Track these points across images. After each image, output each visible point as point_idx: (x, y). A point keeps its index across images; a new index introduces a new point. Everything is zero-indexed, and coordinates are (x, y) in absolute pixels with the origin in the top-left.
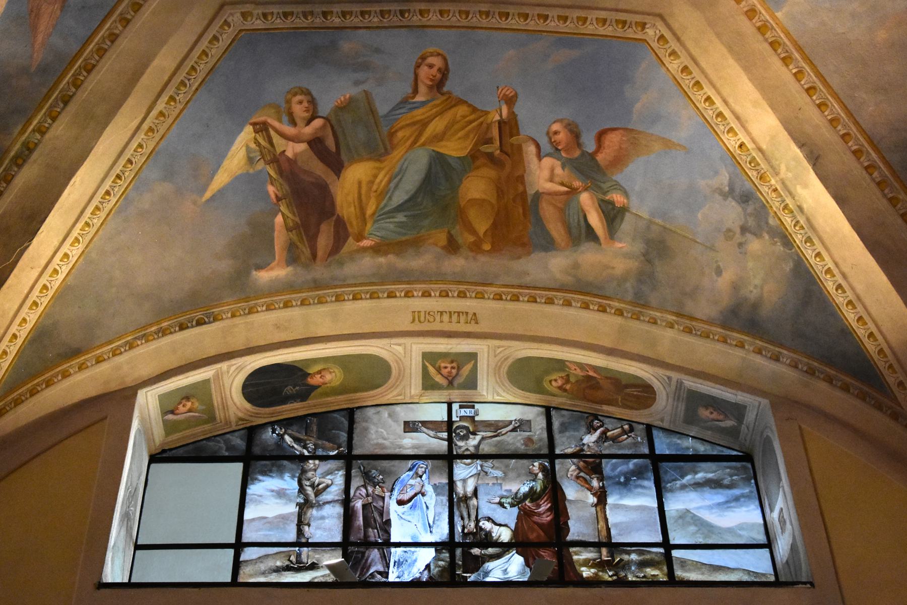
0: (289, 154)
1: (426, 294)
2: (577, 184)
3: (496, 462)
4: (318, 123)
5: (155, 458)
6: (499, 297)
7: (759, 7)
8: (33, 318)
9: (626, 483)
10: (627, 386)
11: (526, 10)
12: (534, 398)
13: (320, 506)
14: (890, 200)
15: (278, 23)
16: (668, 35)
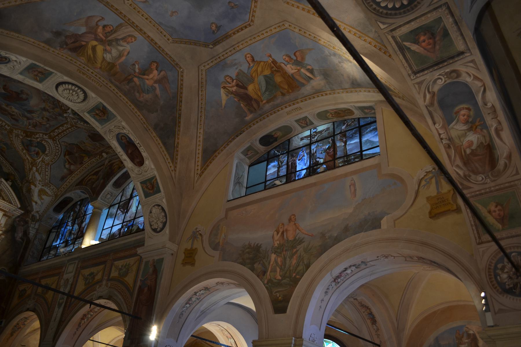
0: (234, 90)
1: (286, 107)
2: (298, 68)
3: (321, 142)
4: (235, 81)
5: (250, 166)
6: (302, 101)
7: (304, 7)
8: (201, 148)
9: (352, 138)
10: (345, 111)
11: (258, 34)
12: (329, 121)
13: (282, 166)
14: (364, 40)
15: (212, 64)
16: (291, 24)
